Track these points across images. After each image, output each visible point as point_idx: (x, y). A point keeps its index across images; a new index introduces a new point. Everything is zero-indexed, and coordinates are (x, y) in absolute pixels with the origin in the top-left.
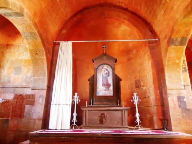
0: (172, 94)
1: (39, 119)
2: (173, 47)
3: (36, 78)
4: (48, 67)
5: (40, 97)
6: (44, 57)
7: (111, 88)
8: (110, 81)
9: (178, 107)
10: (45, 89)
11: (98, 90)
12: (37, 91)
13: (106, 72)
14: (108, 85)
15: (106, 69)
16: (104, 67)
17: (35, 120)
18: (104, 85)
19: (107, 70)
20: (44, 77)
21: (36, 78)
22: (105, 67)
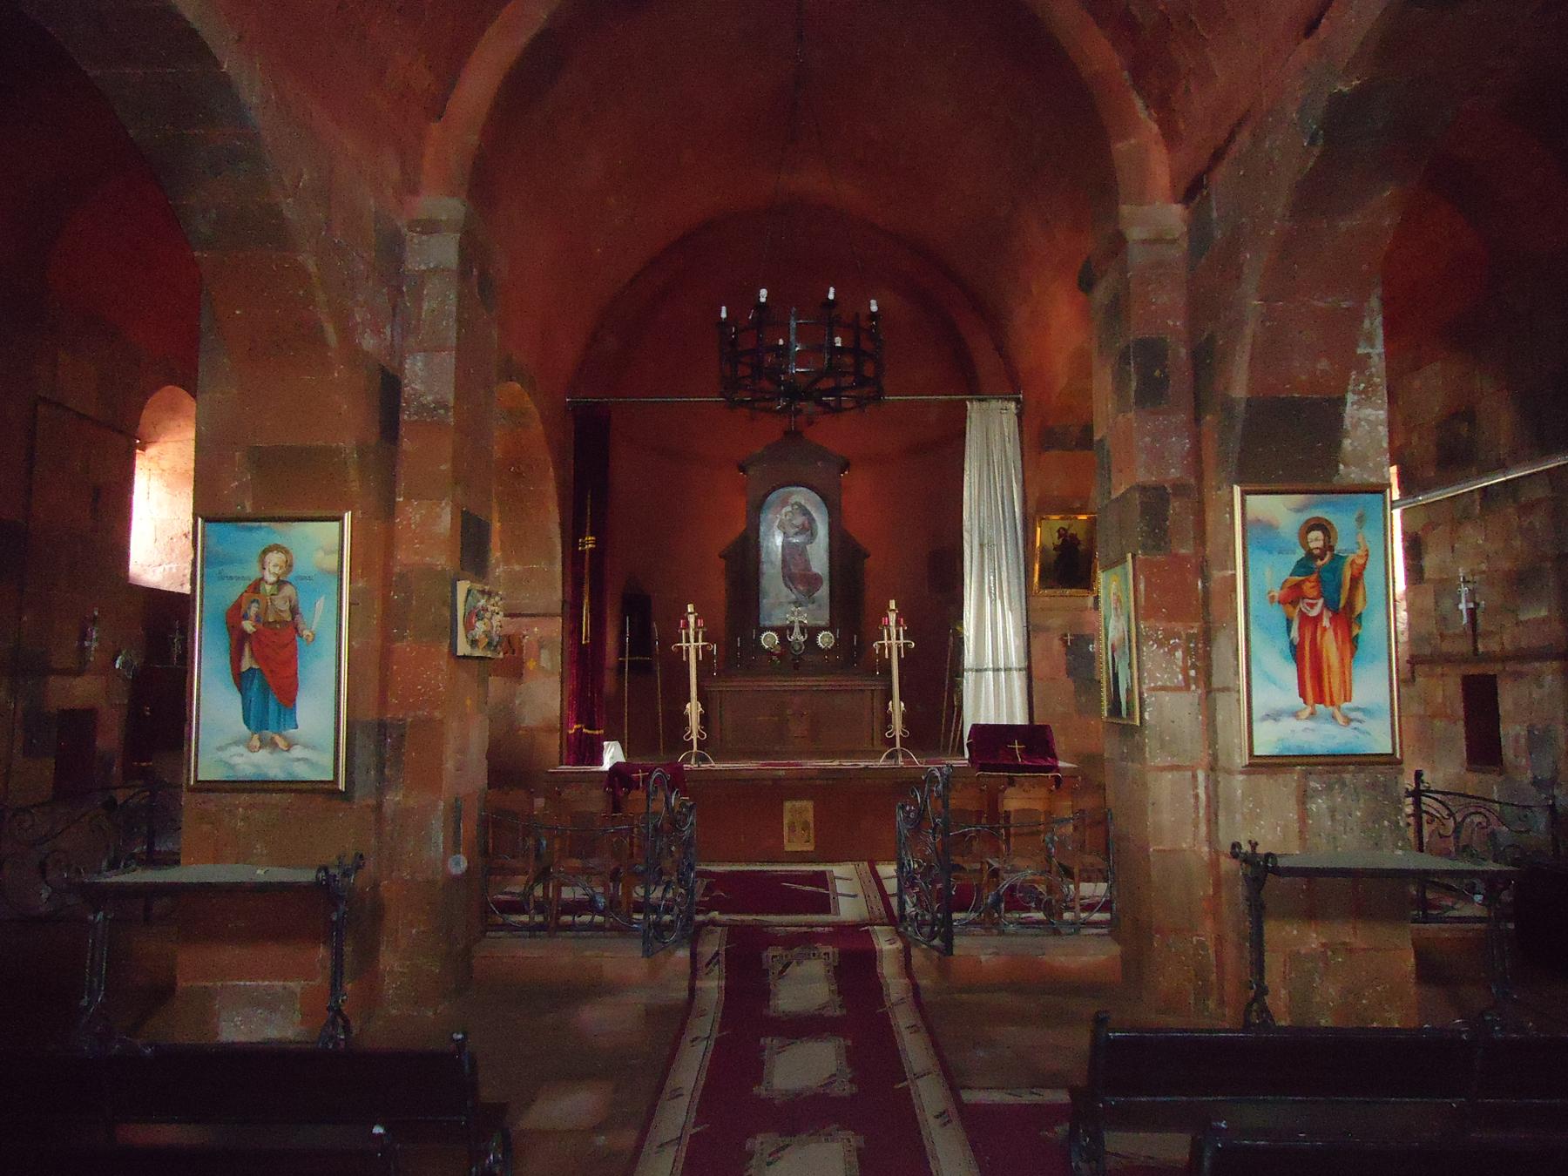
0: (1047, 629)
1: (549, 730)
2: (1054, 453)
3: (517, 568)
4: (562, 525)
5: (541, 647)
6: (551, 488)
7: (823, 592)
8: (818, 557)
9: (1063, 672)
10: (553, 615)
11: (765, 603)
12: (525, 620)
13: (799, 520)
14: (812, 581)
15: (800, 506)
16: (795, 498)
17: (530, 730)
18: (789, 578)
19: (806, 513)
20: (551, 563)
21: (517, 568)
22: (801, 496)
